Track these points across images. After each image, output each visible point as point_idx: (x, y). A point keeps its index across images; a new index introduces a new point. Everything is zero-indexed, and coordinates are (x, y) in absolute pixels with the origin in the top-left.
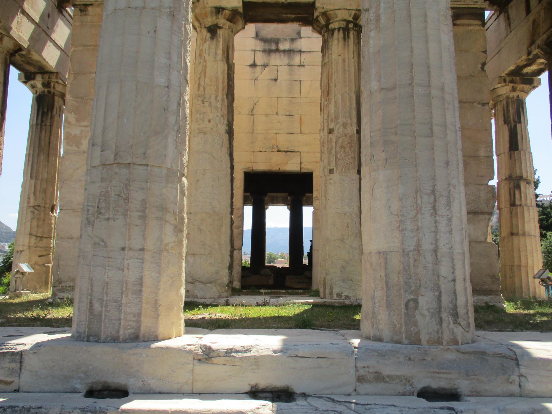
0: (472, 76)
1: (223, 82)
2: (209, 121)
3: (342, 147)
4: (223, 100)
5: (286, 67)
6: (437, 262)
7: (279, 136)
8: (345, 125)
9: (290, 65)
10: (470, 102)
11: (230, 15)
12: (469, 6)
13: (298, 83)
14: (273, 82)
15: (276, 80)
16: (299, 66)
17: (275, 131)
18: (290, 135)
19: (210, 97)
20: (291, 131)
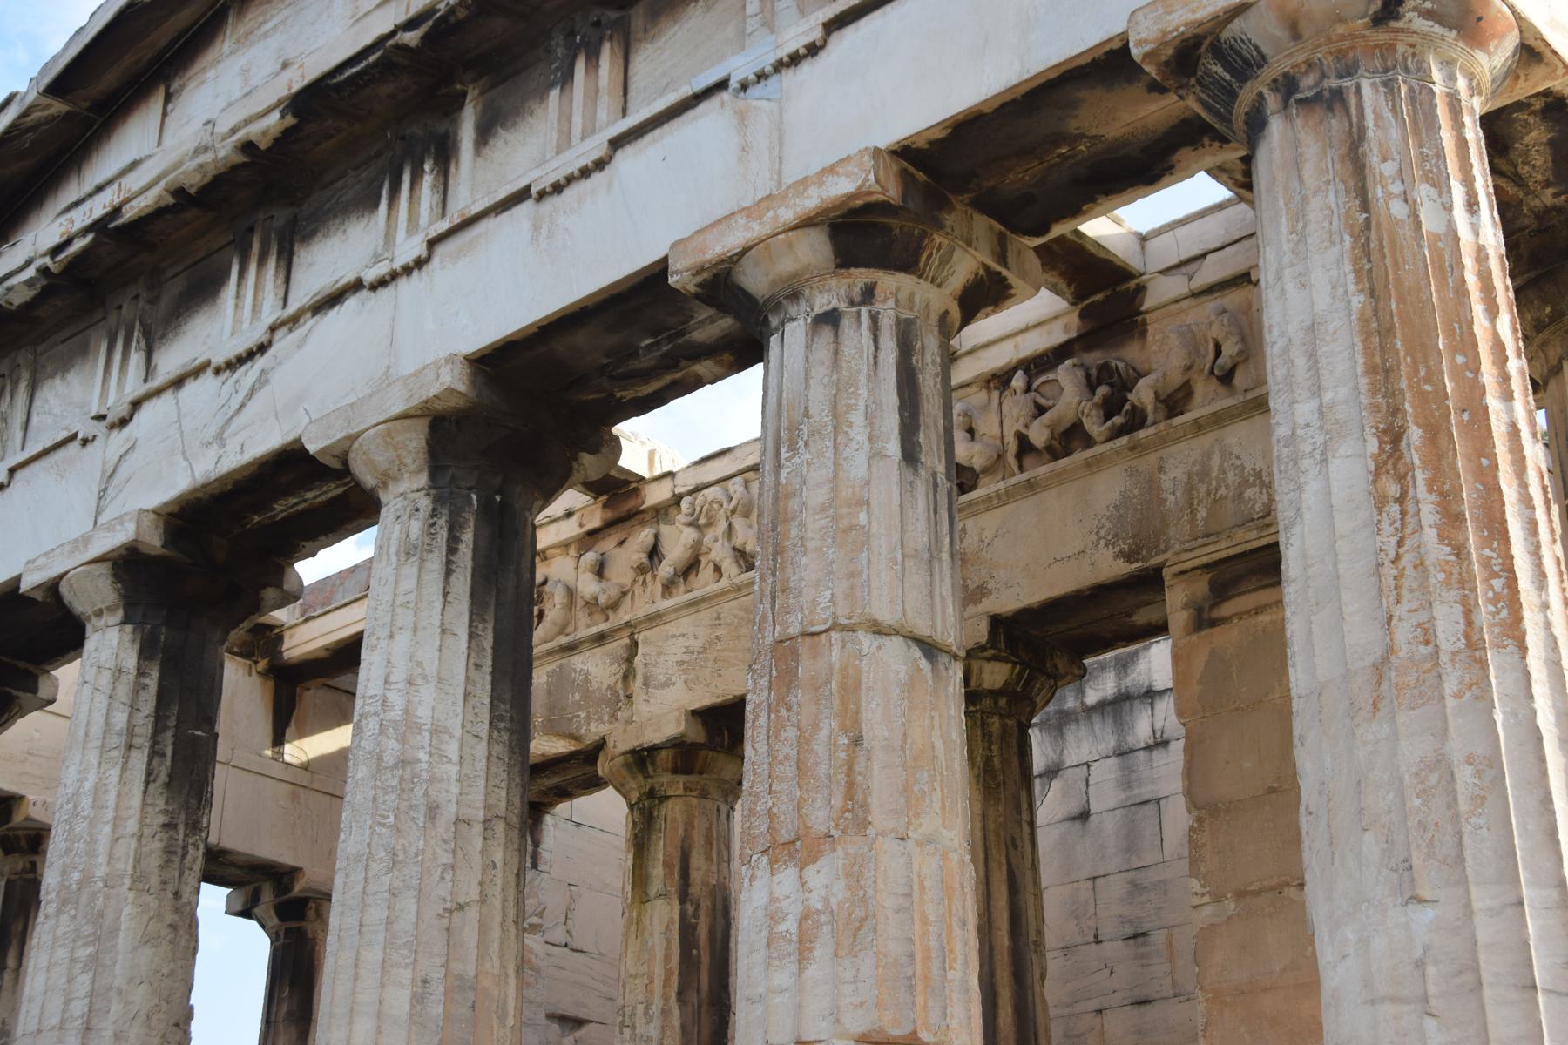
0: (1272, 791)
1: (667, 958)
4: (665, 1013)
5: (1113, 761)
7: (1108, 1015)
9: (1123, 753)
10: (1272, 888)
11: (675, 758)
12: (1249, 547)
13: (1152, 807)
14: (1078, 824)
15: (1084, 816)
16: (1148, 748)
17: (1094, 1004)
18: (1143, 1009)
20: (1142, 993)
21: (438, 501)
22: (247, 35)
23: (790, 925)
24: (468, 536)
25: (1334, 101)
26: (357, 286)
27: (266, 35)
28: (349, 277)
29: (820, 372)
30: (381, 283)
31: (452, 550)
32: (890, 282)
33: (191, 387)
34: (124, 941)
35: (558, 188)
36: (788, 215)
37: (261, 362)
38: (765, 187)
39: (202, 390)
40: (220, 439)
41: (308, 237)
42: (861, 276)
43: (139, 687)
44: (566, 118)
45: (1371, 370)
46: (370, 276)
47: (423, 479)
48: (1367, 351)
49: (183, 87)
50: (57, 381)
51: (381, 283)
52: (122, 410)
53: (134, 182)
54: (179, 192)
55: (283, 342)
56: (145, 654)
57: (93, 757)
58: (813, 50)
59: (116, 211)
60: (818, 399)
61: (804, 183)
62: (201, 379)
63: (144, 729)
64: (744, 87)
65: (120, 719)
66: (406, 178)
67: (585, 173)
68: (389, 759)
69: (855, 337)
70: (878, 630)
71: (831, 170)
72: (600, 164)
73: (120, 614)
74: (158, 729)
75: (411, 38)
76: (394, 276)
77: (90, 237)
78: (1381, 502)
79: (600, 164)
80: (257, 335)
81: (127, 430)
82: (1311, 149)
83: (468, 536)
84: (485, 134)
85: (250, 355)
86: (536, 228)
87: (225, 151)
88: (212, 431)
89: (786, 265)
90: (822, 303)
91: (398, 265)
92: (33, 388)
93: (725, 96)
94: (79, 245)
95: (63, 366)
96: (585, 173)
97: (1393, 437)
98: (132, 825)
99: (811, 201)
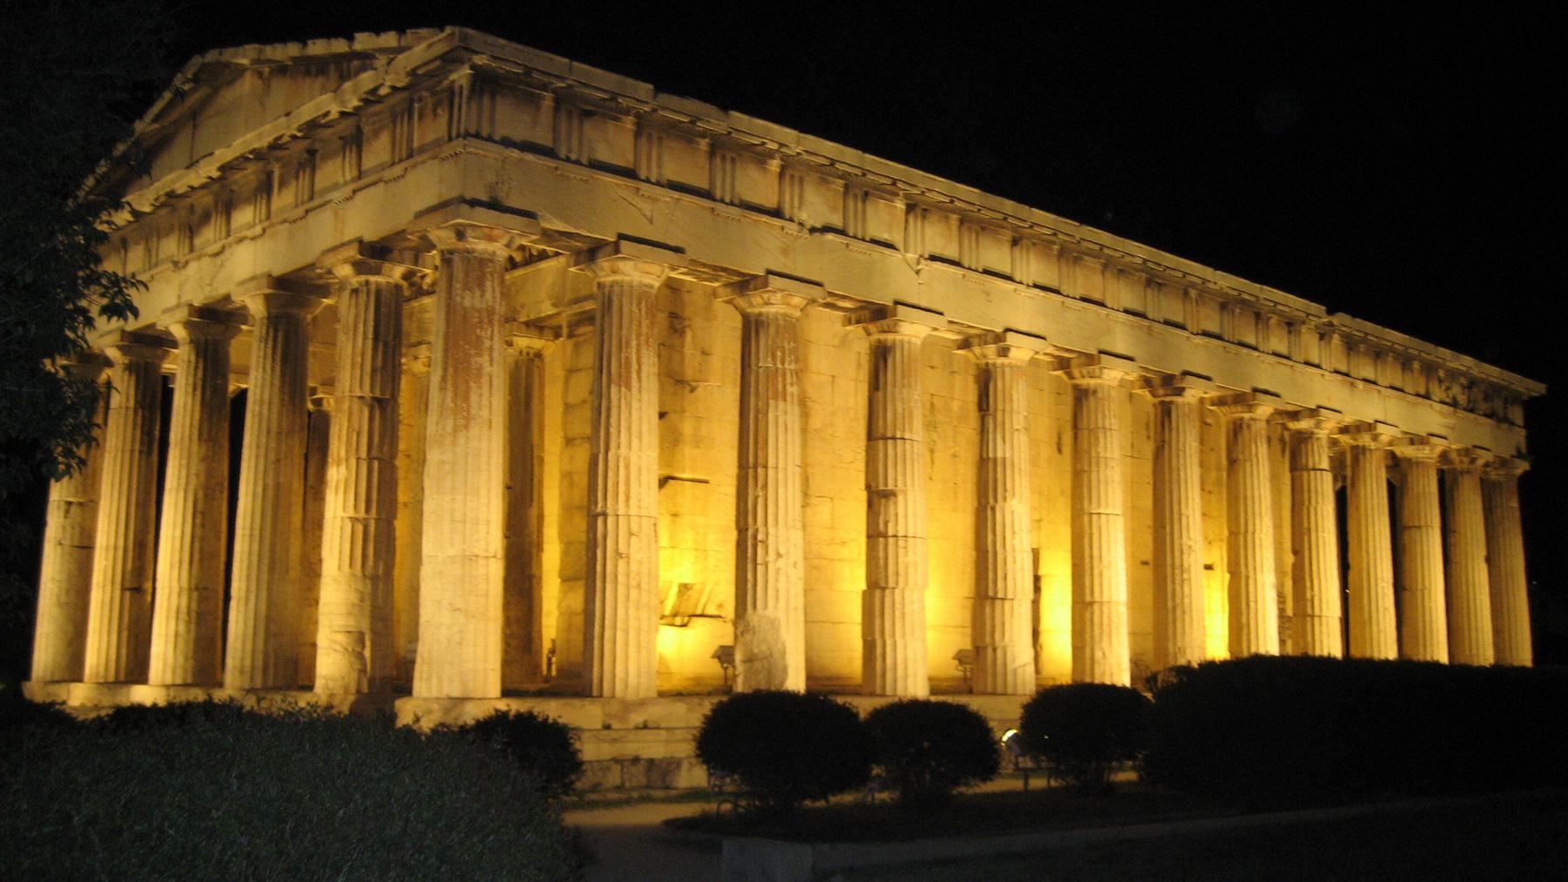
24: (280, 334)
29: (353, 310)
31: (275, 341)
32: (373, 279)
34: (195, 460)
37: (222, 257)
39: (206, 261)
42: (363, 278)
43: (196, 368)
56: (197, 355)
60: (351, 320)
63: (200, 383)
69: (363, 297)
74: (204, 381)
83: (280, 334)
97: (445, 370)
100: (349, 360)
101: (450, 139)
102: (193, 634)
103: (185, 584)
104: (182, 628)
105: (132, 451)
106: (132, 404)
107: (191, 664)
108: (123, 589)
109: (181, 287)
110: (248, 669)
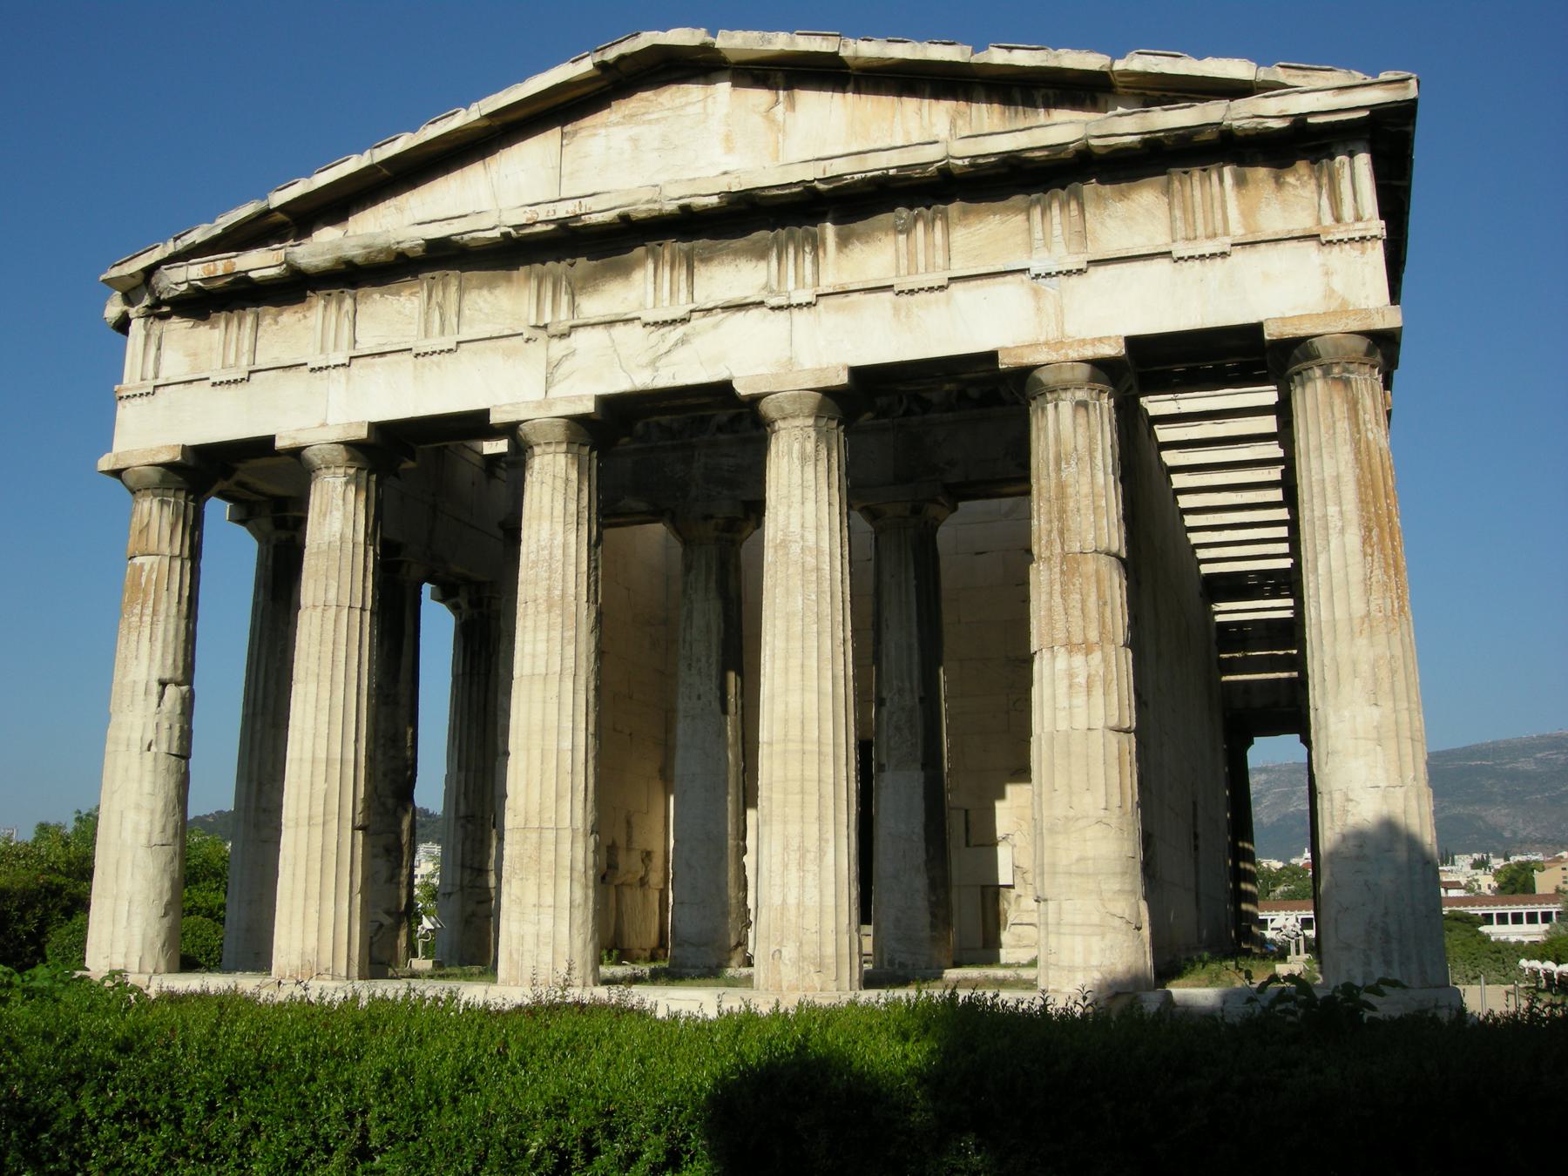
2: (699, 697)
3: (898, 728)
6: (801, 915)
8: (901, 691)
19: (699, 660)
21: (818, 432)
22: (632, 116)
23: (1081, 680)
25: (1347, 383)
26: (761, 303)
27: (650, 122)
28: (758, 299)
29: (1080, 430)
30: (780, 308)
33: (619, 330)
35: (911, 292)
36: (1074, 355)
37: (681, 330)
38: (1052, 334)
40: (653, 364)
41: (706, 260)
43: (579, 490)
44: (912, 255)
45: (1361, 501)
46: (774, 302)
47: (811, 421)
48: (1360, 493)
49: (575, 133)
50: (485, 292)
51: (780, 308)
52: (564, 328)
53: (589, 204)
54: (625, 218)
55: (698, 322)
57: (559, 528)
58: (1080, 271)
59: (577, 217)
60: (1082, 442)
61: (1083, 342)
62: (630, 326)
64: (1038, 276)
65: (573, 507)
66: (791, 250)
67: (931, 289)
68: (808, 567)
70: (1108, 554)
71: (1100, 340)
72: (941, 288)
73: (564, 447)
75: (821, 186)
76: (790, 306)
77: (551, 227)
78: (1365, 555)
79: (941, 288)
80: (680, 312)
81: (565, 342)
82: (1337, 401)
83: (835, 454)
84: (843, 242)
85: (674, 322)
86: (896, 310)
87: (671, 207)
88: (645, 359)
89: (1067, 376)
90: (1081, 395)
91: (794, 302)
92: (461, 291)
93: (1025, 277)
94: (539, 228)
95: (491, 286)
96: (931, 289)
98: (585, 568)
99: (1089, 353)
100: (1085, 503)
101: (1338, 220)
102: (591, 904)
103: (579, 823)
104: (579, 895)
105: (363, 609)
106: (361, 537)
107: (591, 947)
108: (354, 828)
109: (553, 367)
110: (830, 961)
